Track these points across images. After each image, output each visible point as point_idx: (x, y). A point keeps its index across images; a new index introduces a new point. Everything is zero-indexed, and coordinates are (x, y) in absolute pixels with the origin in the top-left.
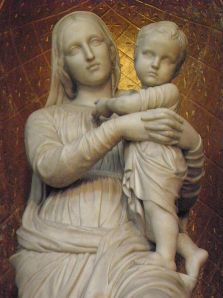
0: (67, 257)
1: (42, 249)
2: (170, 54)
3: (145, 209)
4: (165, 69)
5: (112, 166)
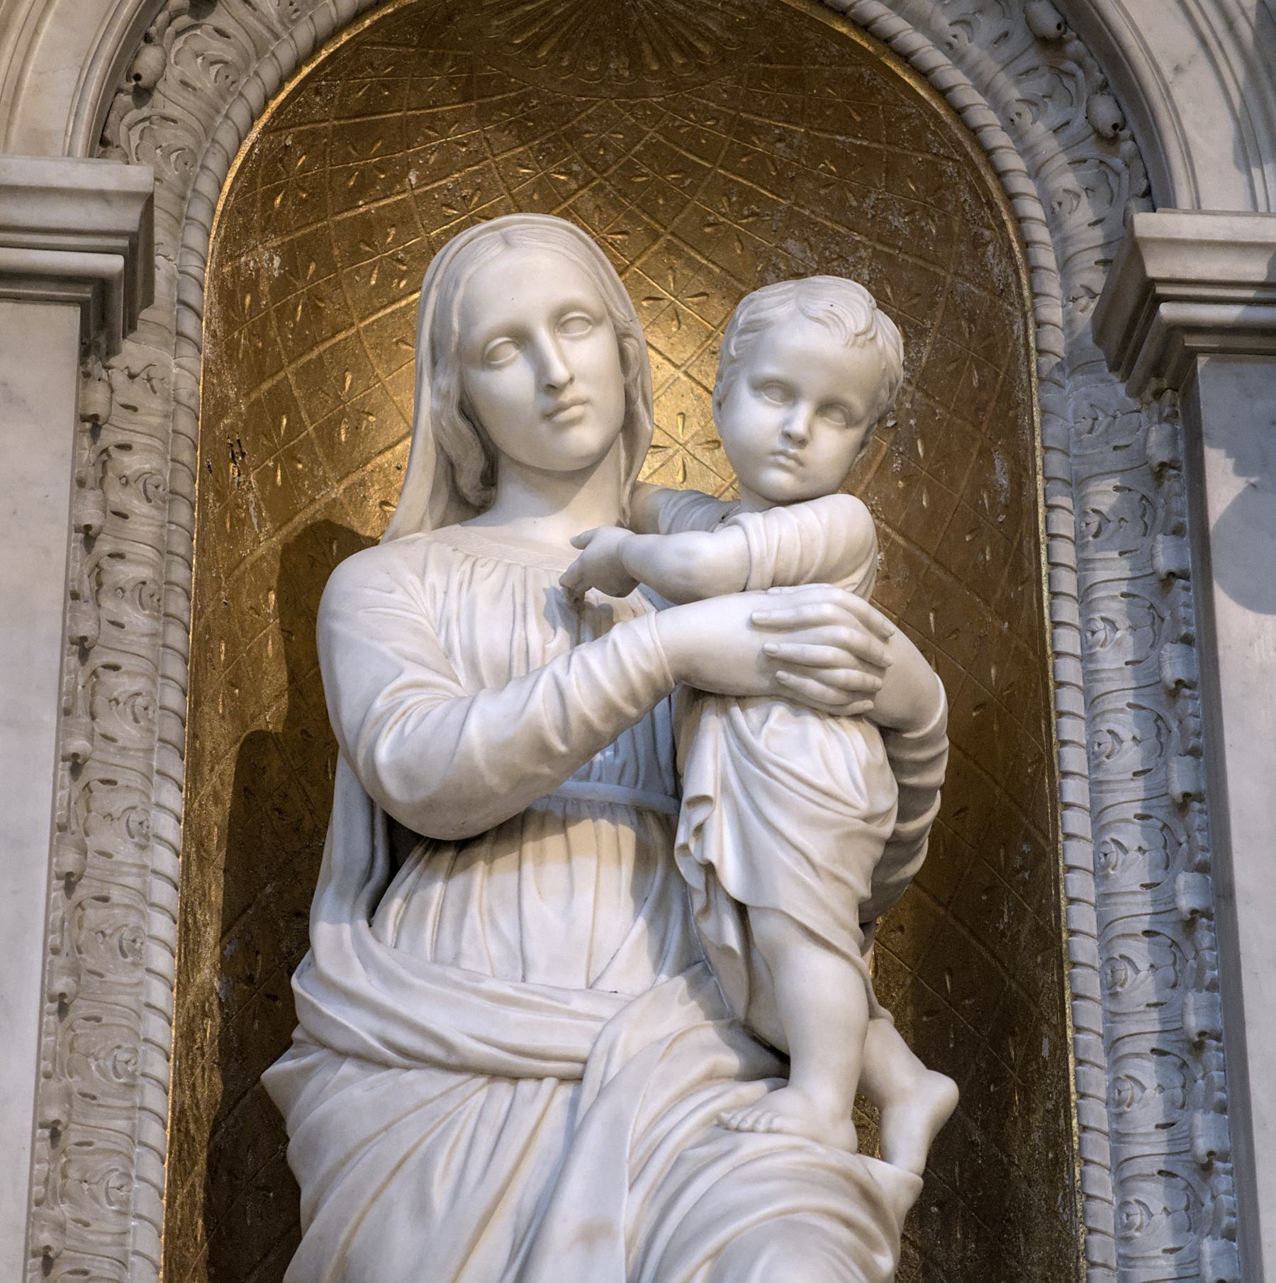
0: (480, 1089)
1: (389, 1054)
2: (857, 403)
3: (756, 937)
4: (831, 444)
5: (630, 771)
